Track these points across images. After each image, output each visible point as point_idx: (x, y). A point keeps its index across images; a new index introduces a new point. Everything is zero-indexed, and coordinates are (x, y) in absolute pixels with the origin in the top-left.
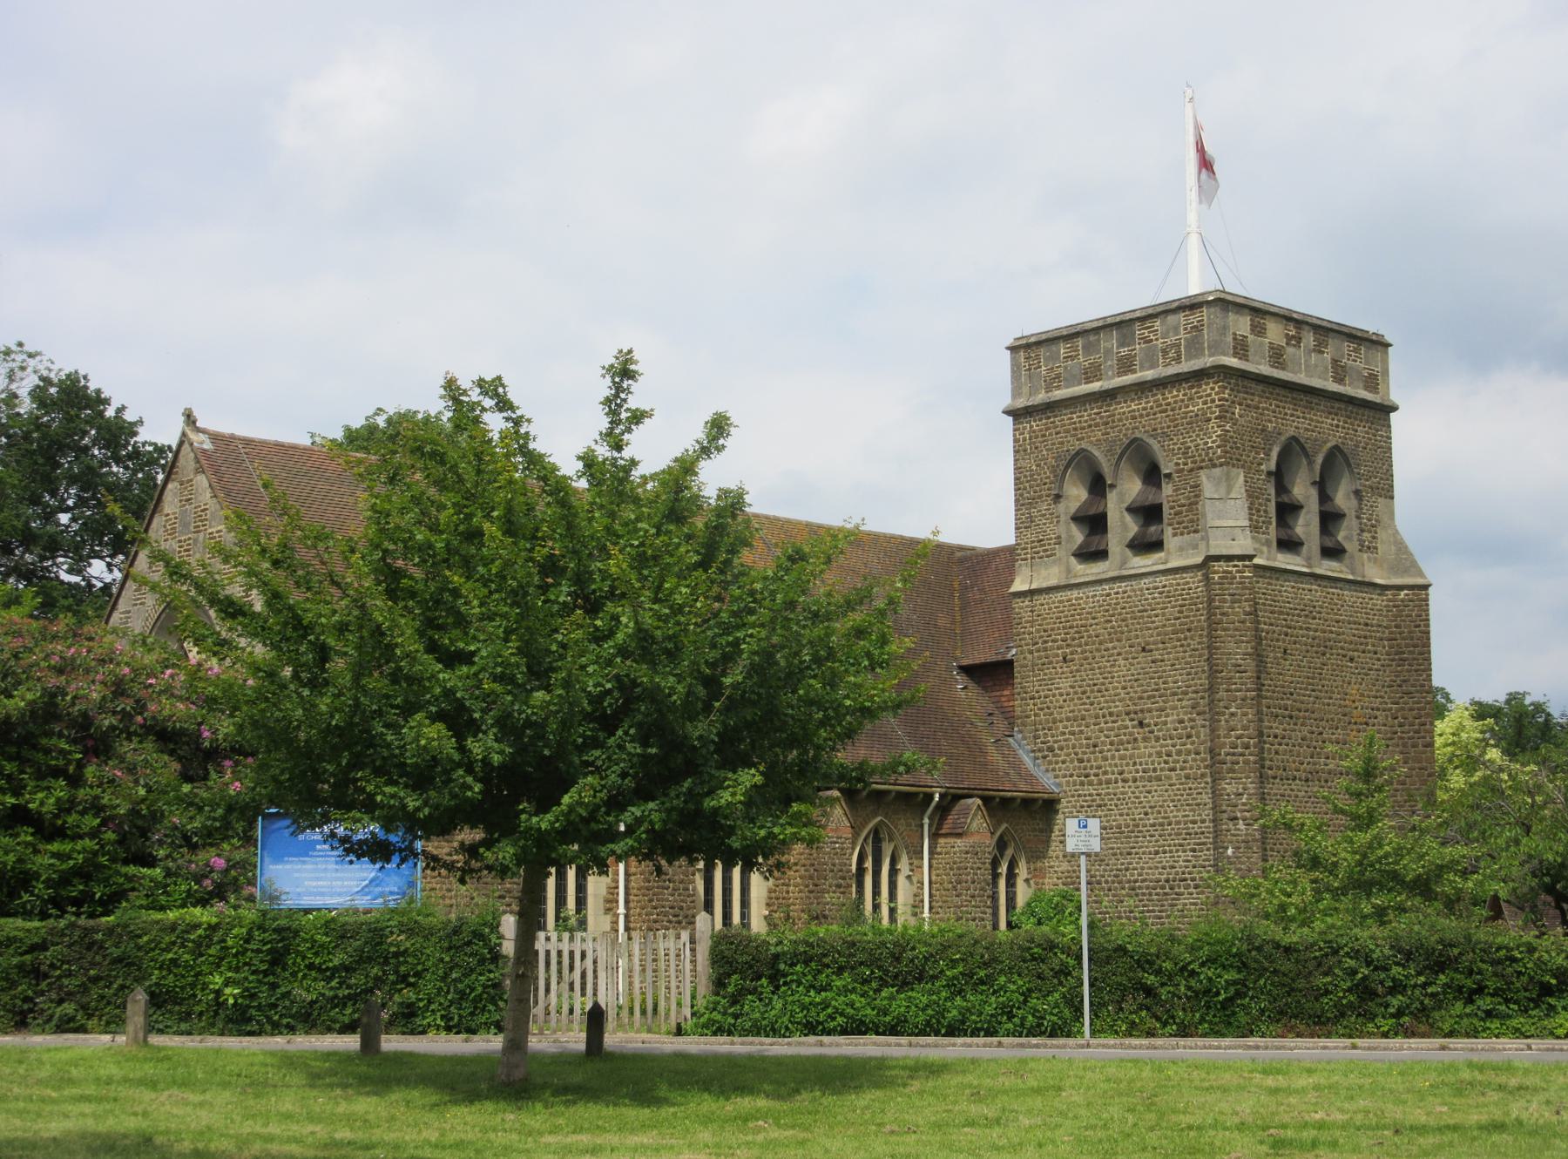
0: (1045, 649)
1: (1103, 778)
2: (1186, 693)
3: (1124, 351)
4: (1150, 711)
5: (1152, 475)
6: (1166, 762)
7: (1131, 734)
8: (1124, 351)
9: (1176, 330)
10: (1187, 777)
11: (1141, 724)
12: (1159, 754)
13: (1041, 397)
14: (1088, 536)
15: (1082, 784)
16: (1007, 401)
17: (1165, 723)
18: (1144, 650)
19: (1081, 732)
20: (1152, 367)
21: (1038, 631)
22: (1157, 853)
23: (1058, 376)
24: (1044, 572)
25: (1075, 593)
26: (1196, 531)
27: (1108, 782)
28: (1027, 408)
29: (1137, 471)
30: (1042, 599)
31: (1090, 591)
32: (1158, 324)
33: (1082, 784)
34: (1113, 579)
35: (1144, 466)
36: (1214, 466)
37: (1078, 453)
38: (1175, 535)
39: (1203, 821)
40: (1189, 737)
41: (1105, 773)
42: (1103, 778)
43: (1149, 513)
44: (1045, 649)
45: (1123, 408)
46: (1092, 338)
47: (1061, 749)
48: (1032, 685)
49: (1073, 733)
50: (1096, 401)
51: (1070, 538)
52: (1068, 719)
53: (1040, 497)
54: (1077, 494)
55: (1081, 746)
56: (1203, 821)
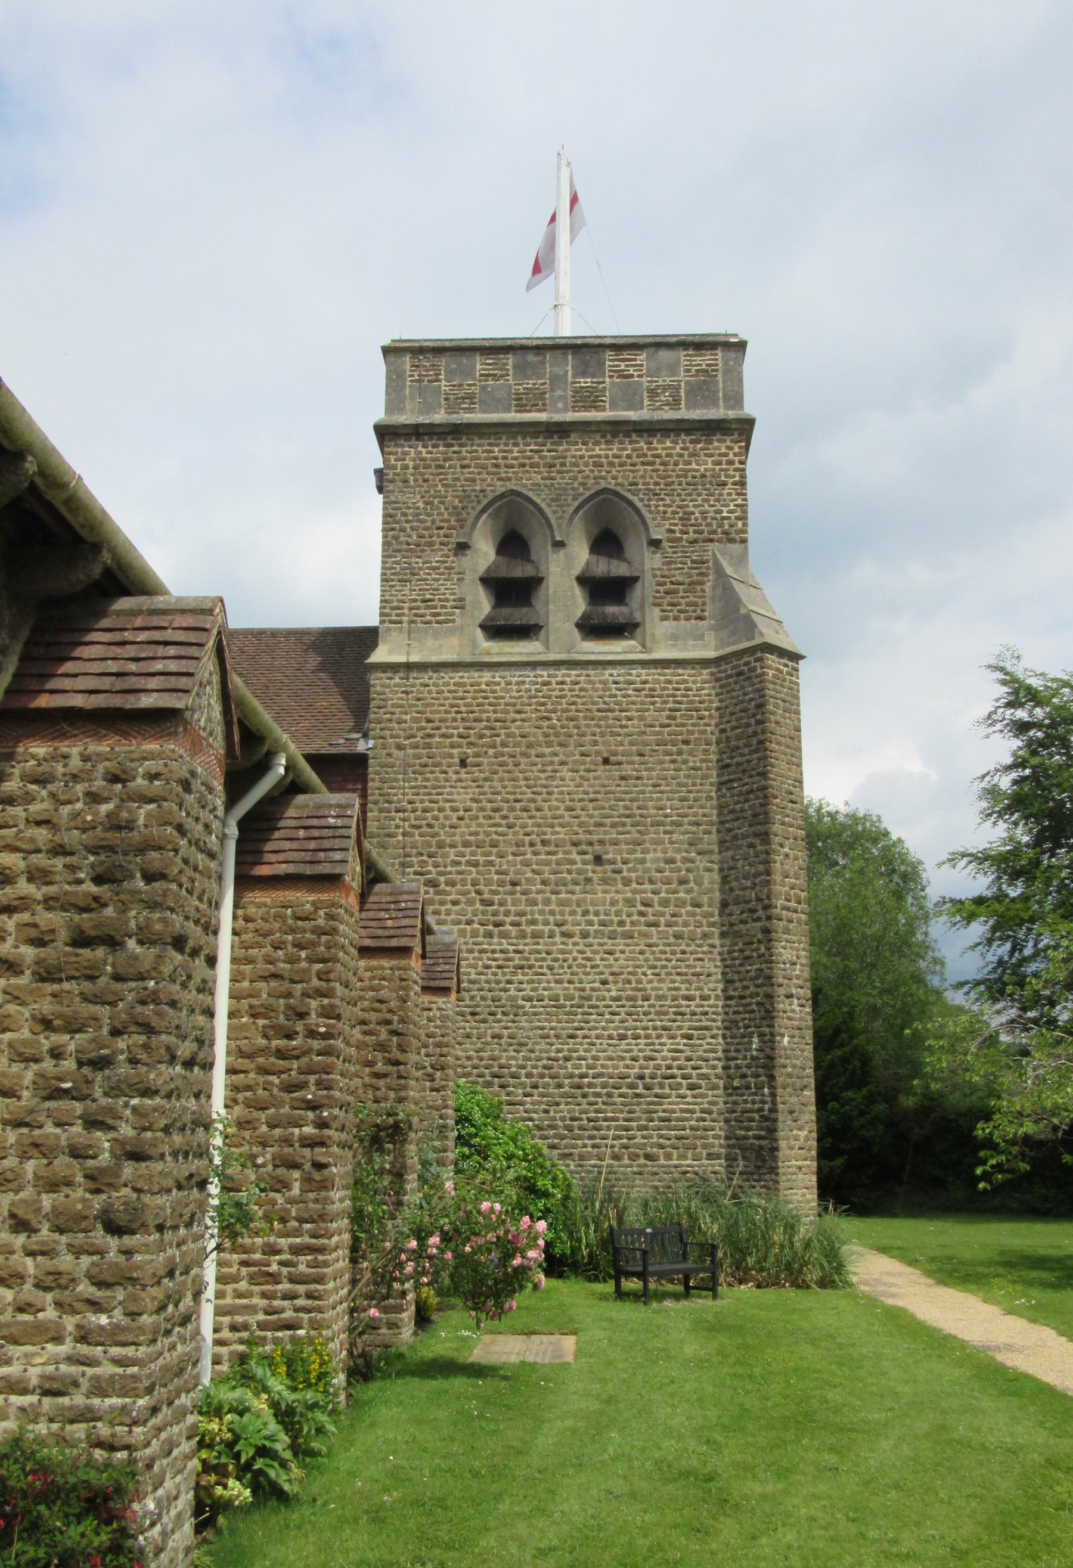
0: (429, 746)
1: (529, 929)
2: (680, 824)
3: (585, 382)
4: (616, 843)
5: (607, 542)
6: (641, 914)
7: (580, 872)
8: (585, 382)
9: (673, 370)
10: (678, 936)
11: (598, 860)
12: (630, 902)
13: (439, 417)
14: (494, 607)
15: (489, 935)
16: (379, 414)
17: (643, 861)
18: (606, 761)
19: (491, 863)
20: (630, 408)
21: (416, 720)
22: (622, 1037)
23: (470, 397)
24: (430, 642)
25: (487, 676)
26: (700, 618)
27: (536, 935)
28: (417, 426)
29: (588, 532)
30: (420, 679)
31: (514, 676)
32: (642, 358)
33: (489, 935)
34: (557, 664)
35: (596, 531)
36: (732, 541)
37: (502, 496)
38: (665, 618)
39: (703, 998)
40: (682, 882)
41: (533, 922)
42: (529, 929)
43: (604, 590)
44: (429, 746)
45: (576, 450)
46: (531, 358)
47: (453, 884)
48: (402, 791)
49: (476, 864)
50: (536, 435)
51: (477, 604)
52: (466, 844)
53: (430, 544)
54: (485, 552)
55: (488, 882)
56: (703, 998)
